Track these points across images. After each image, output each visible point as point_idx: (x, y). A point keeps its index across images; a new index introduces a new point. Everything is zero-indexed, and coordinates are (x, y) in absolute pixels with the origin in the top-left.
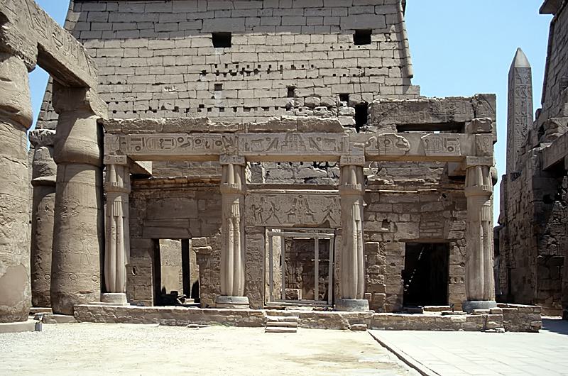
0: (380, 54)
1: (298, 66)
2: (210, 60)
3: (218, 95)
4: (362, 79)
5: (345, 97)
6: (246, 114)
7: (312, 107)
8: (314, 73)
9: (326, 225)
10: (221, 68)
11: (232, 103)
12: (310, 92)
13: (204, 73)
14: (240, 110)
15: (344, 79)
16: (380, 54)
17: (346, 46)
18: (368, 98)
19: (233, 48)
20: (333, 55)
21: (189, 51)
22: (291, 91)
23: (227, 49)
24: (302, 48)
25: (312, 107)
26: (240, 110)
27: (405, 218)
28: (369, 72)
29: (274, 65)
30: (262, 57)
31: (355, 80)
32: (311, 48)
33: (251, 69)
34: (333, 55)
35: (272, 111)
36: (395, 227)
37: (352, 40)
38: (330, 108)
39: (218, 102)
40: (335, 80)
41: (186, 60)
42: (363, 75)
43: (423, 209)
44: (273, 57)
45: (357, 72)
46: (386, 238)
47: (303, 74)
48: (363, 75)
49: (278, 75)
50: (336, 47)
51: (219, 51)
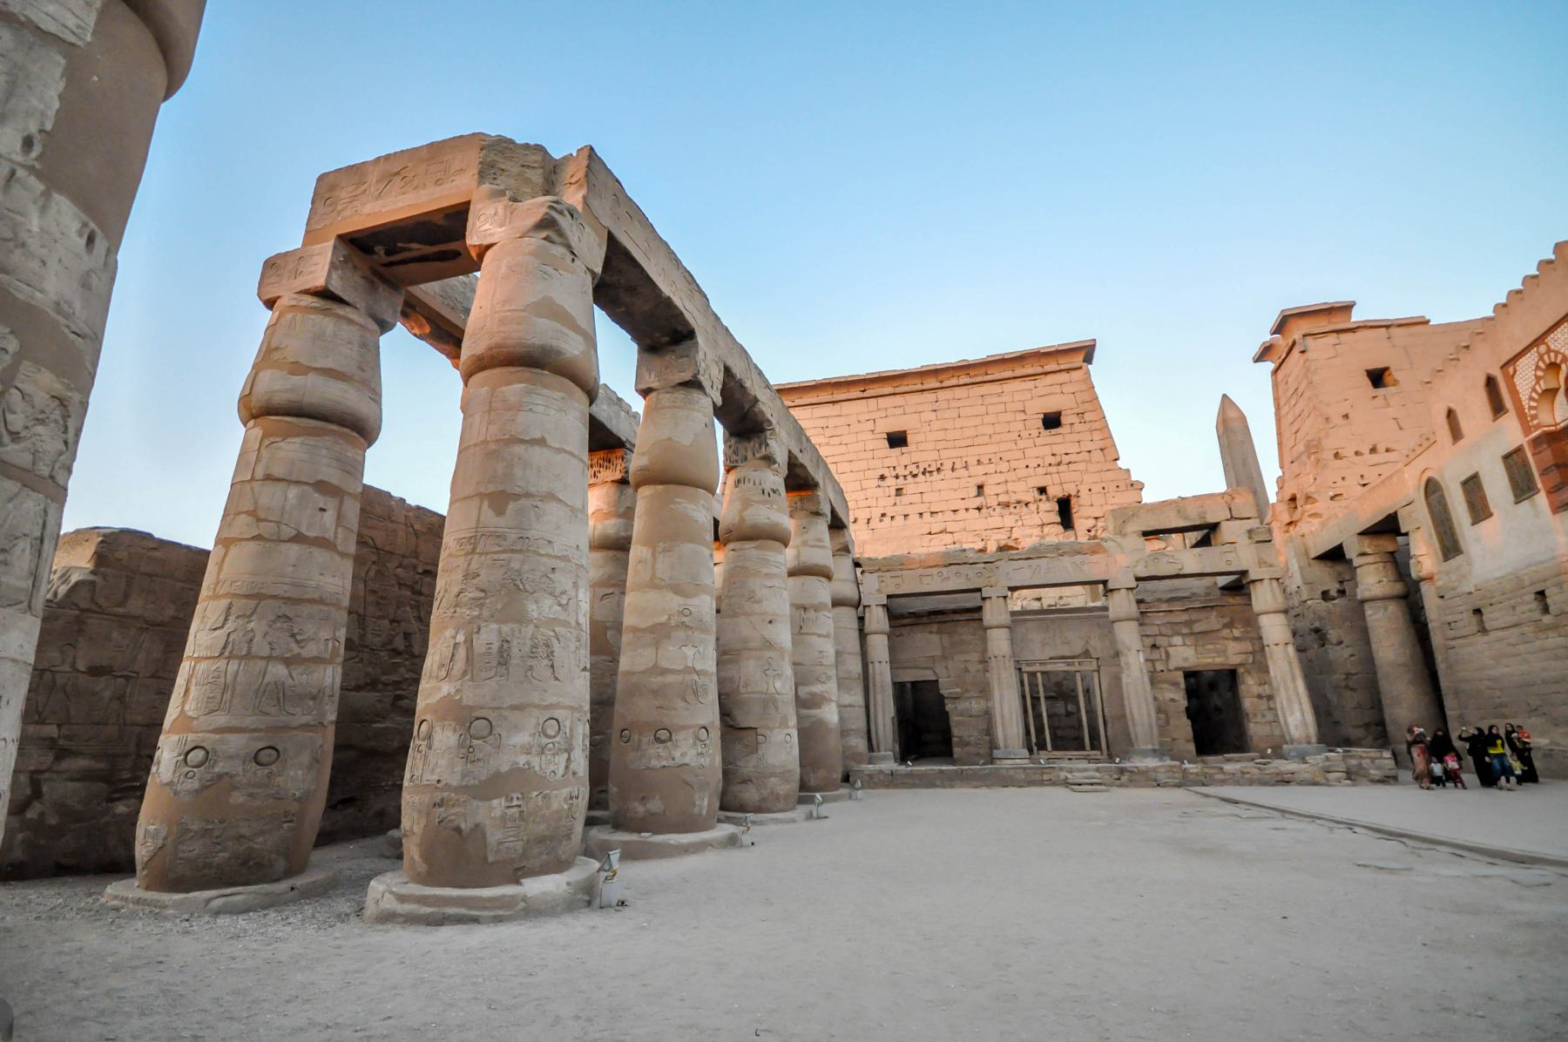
0: (1076, 437)
1: (985, 460)
2: (889, 462)
3: (905, 499)
4: (1063, 468)
5: (1042, 490)
6: (932, 520)
7: (1007, 505)
8: (1004, 466)
9: (1086, 654)
10: (901, 471)
11: (922, 508)
12: (1000, 489)
13: (882, 477)
14: (927, 516)
19: (912, 447)
20: (1021, 444)
21: (863, 455)
22: (980, 487)
23: (904, 449)
24: (987, 439)
25: (1007, 505)
26: (927, 516)
27: (1177, 640)
28: (1066, 459)
29: (958, 462)
30: (944, 454)
31: (1053, 469)
32: (996, 438)
33: (933, 468)
34: (1021, 444)
35: (962, 514)
36: (1167, 653)
37: (1041, 424)
39: (900, 510)
40: (1030, 470)
41: (863, 465)
43: (1197, 628)
44: (954, 453)
45: (1053, 460)
46: (1159, 666)
47: (991, 468)
49: (964, 473)
50: (1025, 434)
51: (897, 451)
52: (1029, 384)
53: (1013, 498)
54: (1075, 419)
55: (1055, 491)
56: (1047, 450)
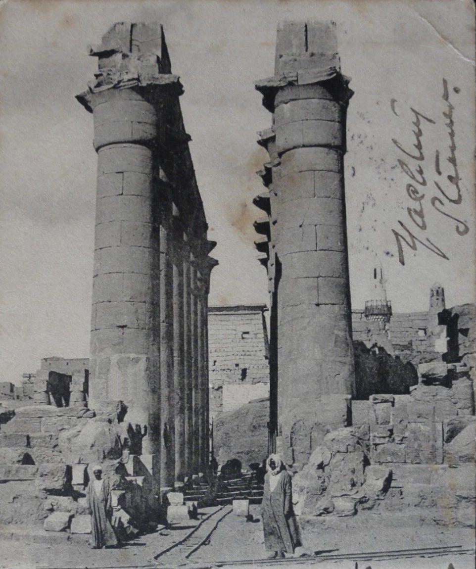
4: (245, 357)
5: (237, 365)
7: (224, 370)
8: (224, 354)
15: (238, 357)
16: (252, 344)
17: (238, 341)
18: (247, 366)
25: (224, 370)
28: (248, 353)
31: (242, 357)
38: (231, 370)
40: (233, 357)
42: (245, 355)
45: (243, 353)
47: (220, 354)
48: (245, 355)
50: (234, 341)
52: (240, 318)
53: (226, 368)
54: (253, 336)
55: (242, 366)
56: (242, 348)
